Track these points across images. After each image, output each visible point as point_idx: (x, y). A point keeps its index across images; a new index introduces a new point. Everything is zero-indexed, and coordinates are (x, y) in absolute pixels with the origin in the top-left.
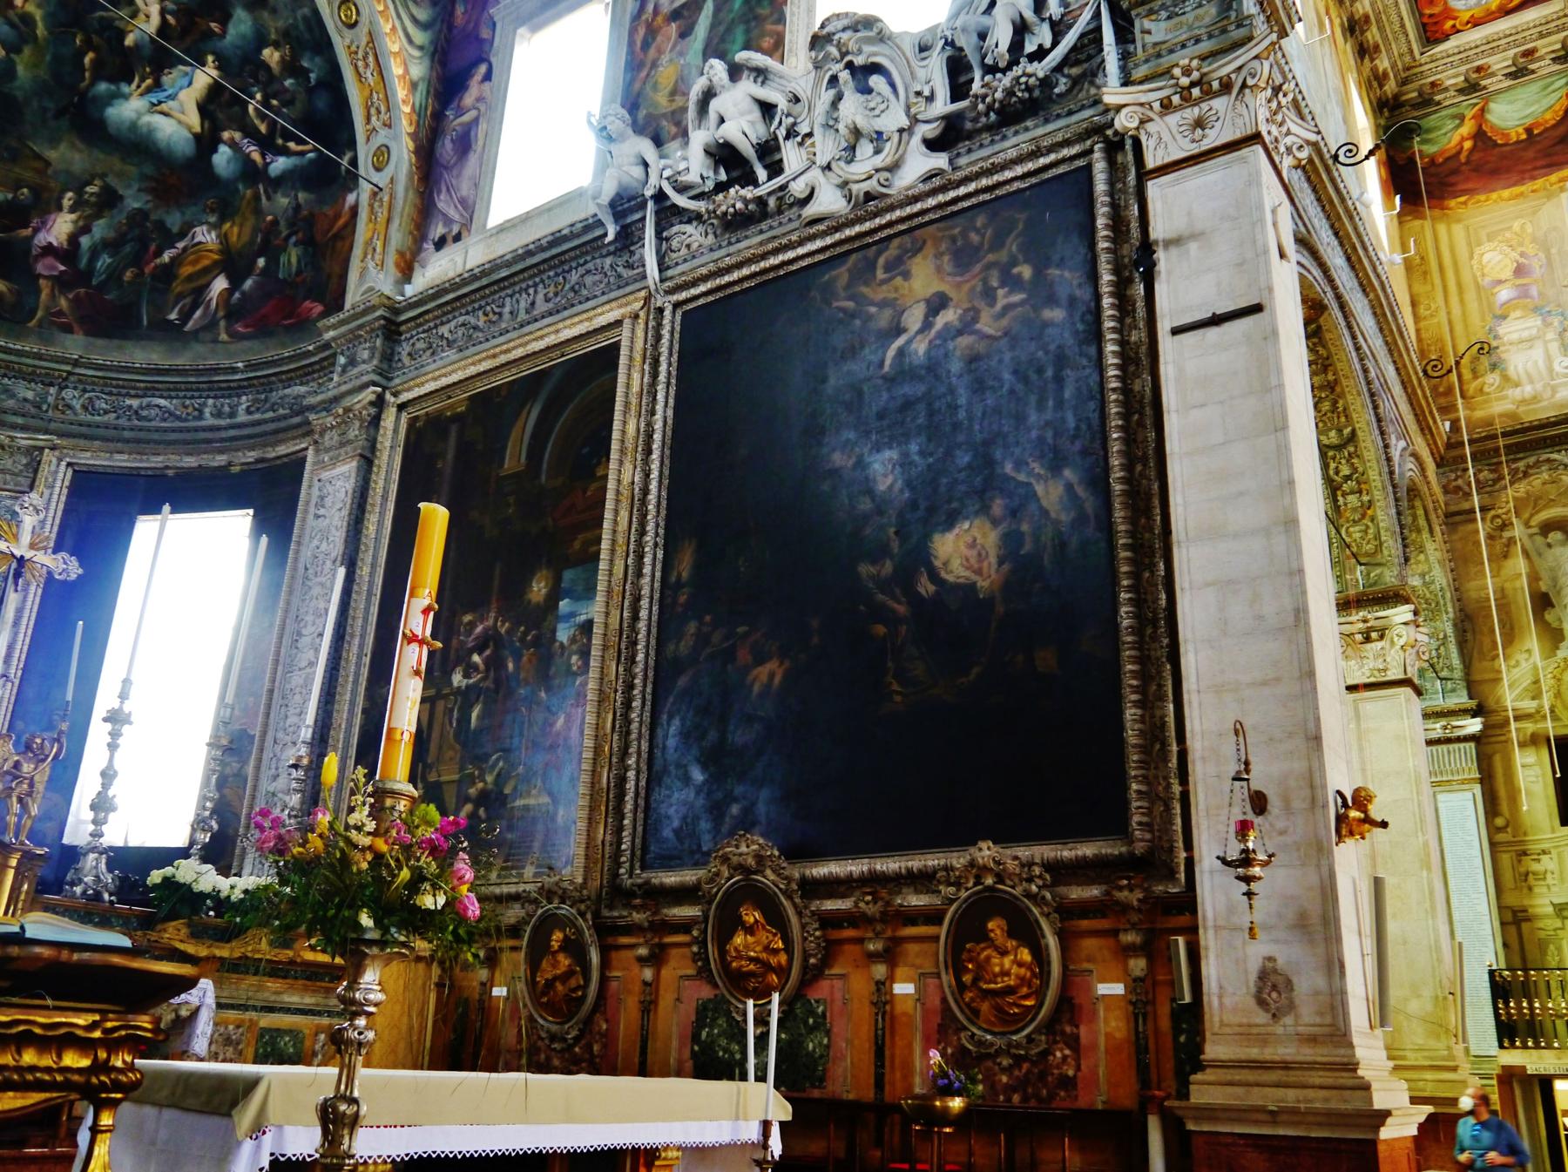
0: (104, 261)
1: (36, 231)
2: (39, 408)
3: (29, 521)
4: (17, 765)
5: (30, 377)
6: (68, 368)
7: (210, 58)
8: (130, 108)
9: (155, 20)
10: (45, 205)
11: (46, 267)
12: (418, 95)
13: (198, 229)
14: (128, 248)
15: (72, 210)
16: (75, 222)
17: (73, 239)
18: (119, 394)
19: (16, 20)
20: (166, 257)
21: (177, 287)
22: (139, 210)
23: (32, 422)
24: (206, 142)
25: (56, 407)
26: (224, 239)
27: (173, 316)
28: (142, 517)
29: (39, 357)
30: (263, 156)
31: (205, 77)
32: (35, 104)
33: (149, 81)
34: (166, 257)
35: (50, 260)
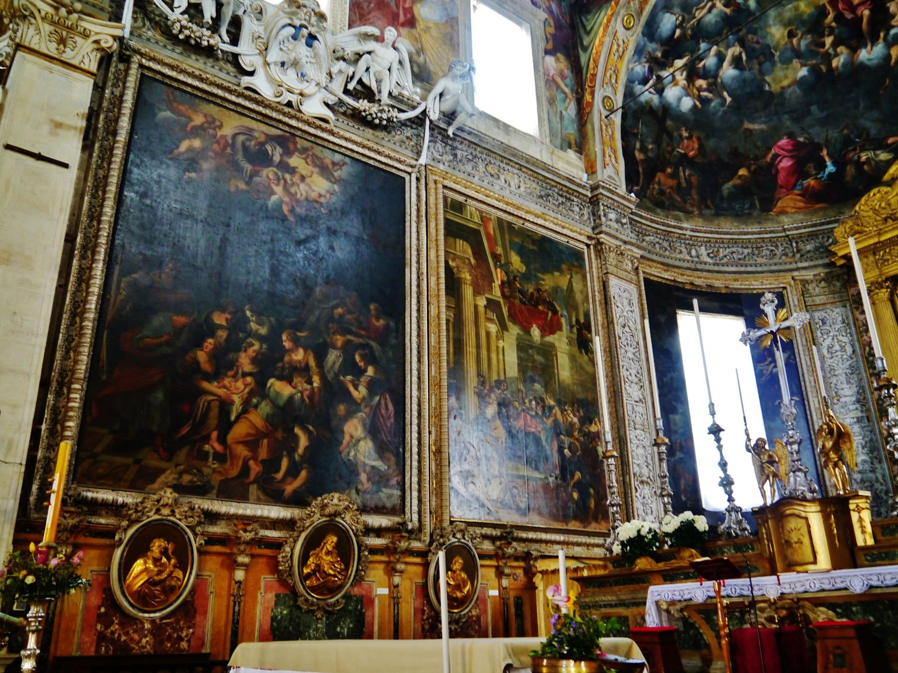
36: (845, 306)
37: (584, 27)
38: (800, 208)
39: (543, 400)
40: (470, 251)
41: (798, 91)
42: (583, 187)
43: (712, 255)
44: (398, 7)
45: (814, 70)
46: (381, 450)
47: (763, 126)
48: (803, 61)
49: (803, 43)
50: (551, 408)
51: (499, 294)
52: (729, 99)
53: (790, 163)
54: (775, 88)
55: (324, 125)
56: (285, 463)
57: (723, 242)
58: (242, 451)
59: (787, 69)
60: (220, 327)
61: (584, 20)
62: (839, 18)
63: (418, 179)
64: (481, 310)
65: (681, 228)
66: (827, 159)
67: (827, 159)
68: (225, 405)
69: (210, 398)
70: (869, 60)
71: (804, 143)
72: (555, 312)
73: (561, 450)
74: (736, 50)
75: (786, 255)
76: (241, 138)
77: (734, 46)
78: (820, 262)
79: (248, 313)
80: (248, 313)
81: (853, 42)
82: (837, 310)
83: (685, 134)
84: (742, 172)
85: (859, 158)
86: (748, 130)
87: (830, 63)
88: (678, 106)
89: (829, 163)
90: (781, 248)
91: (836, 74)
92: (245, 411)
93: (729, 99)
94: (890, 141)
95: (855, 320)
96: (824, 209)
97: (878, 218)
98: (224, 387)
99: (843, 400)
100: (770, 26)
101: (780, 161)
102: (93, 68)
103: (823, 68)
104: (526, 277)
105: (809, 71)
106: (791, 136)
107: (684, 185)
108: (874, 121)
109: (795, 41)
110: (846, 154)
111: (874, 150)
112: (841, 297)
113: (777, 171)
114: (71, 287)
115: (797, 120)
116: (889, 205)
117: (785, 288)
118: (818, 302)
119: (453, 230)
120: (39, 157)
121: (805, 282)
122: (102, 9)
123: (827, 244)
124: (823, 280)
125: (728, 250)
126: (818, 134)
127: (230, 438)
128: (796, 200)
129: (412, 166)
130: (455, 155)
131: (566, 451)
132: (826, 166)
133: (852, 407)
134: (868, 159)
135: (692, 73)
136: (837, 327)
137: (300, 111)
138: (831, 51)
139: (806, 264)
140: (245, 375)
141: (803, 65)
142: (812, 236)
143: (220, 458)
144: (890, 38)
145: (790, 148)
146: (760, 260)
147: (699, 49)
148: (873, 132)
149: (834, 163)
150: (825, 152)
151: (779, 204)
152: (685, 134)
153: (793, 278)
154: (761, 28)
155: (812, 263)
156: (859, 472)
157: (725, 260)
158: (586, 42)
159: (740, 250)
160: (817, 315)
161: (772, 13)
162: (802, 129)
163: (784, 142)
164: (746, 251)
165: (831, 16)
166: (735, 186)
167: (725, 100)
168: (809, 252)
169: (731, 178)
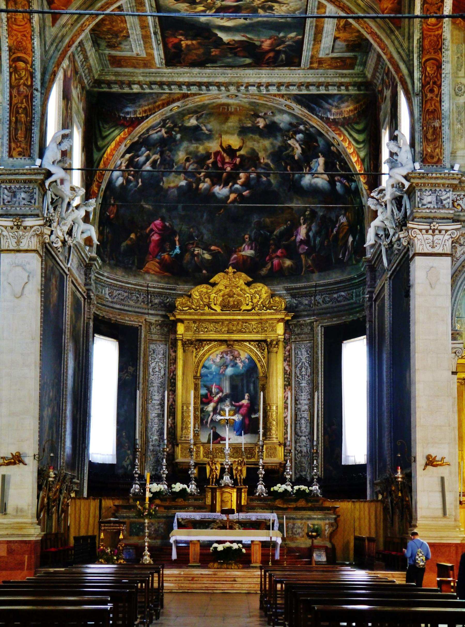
0: (318, 239)
1: (296, 236)
2: (310, 306)
3: (227, 409)
4: (237, 468)
5: (305, 295)
6: (314, 289)
7: (320, 154)
8: (307, 180)
9: (299, 148)
10: (295, 226)
11: (303, 249)
12: (366, 163)
13: (340, 217)
14: (323, 232)
15: (304, 224)
16: (306, 228)
17: (307, 234)
18: (332, 294)
19: (264, 166)
20: (335, 232)
21: (340, 244)
22: (323, 215)
23: (310, 312)
24: (332, 182)
25: (315, 304)
26: (347, 219)
27: (341, 256)
28: (345, 342)
29: (305, 287)
30: (348, 183)
31: (321, 160)
32: (281, 189)
33: (308, 168)
34: (335, 232)
35: (303, 246)
36: (166, 345)
37: (100, 132)
38: (156, 272)
41: (176, 192)
42: (87, 257)
43: (111, 294)
45: (189, 184)
47: (150, 207)
48: (186, 177)
49: (191, 167)
52: (140, 184)
53: (157, 238)
54: (166, 186)
57: (116, 287)
59: (176, 177)
61: (101, 125)
62: (214, 163)
65: (103, 275)
66: (177, 243)
67: (177, 243)
70: (218, 193)
71: (168, 227)
74: (157, 156)
75: (143, 302)
77: (157, 154)
78: (160, 313)
81: (215, 179)
82: (162, 346)
83: (112, 202)
84: (132, 236)
85: (194, 250)
86: (142, 206)
87: (198, 185)
88: (115, 182)
89: (177, 247)
90: (142, 297)
91: (199, 192)
93: (140, 184)
94: (213, 248)
95: (170, 355)
96: (168, 277)
97: (201, 303)
99: (154, 402)
100: (180, 150)
101: (153, 235)
103: (194, 185)
105: (187, 184)
106: (163, 220)
107: (105, 240)
108: (207, 231)
109: (187, 164)
110: (188, 244)
111: (203, 249)
112: (166, 338)
113: (150, 242)
115: (170, 210)
116: (209, 298)
117: (141, 326)
118: (154, 339)
121: (151, 324)
123: (166, 301)
124: (160, 325)
125: (118, 292)
126: (178, 225)
128: (156, 266)
132: (175, 248)
133: (157, 407)
134: (198, 253)
135: (131, 163)
136: (160, 356)
138: (202, 178)
139: (152, 312)
141: (185, 179)
142: (160, 294)
144: (233, 188)
145: (160, 227)
146: (132, 303)
147: (140, 150)
148: (206, 237)
149: (180, 248)
150: (177, 238)
151: (147, 266)
152: (112, 202)
153: (145, 320)
154: (175, 151)
155: (156, 312)
156: (153, 445)
157: (115, 300)
158: (100, 143)
159: (123, 293)
160: (152, 346)
161: (185, 144)
162: (170, 218)
163: (158, 222)
164: (126, 294)
165: (211, 160)
166: (127, 245)
167: (138, 183)
168: (156, 304)
169: (126, 240)
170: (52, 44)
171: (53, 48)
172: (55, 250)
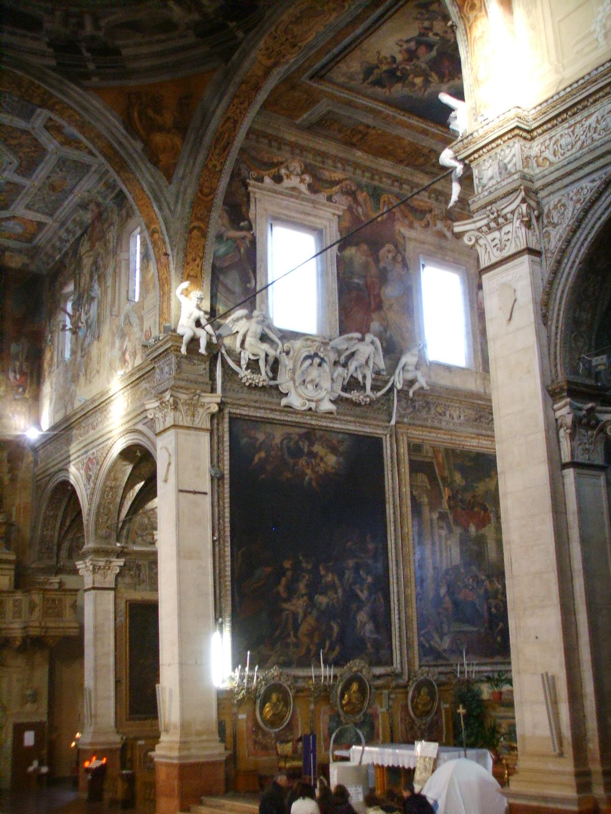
39: (477, 577)
40: (426, 480)
44: (369, 295)
46: (377, 627)
50: (483, 581)
51: (447, 507)
55: (330, 416)
56: (327, 644)
58: (305, 640)
60: (288, 569)
63: (391, 436)
64: (435, 521)
68: (295, 615)
69: (287, 612)
72: (485, 510)
73: (489, 608)
76: (285, 442)
79: (301, 558)
80: (301, 558)
92: (305, 616)
98: (293, 605)
102: (208, 426)
104: (465, 489)
114: (217, 564)
119: (416, 467)
120: (195, 493)
122: (207, 384)
127: (299, 634)
129: (387, 427)
130: (414, 407)
131: (493, 610)
137: (316, 412)
140: (303, 596)
143: (296, 645)
170: (176, 202)
171: (179, 206)
172: (308, 413)
